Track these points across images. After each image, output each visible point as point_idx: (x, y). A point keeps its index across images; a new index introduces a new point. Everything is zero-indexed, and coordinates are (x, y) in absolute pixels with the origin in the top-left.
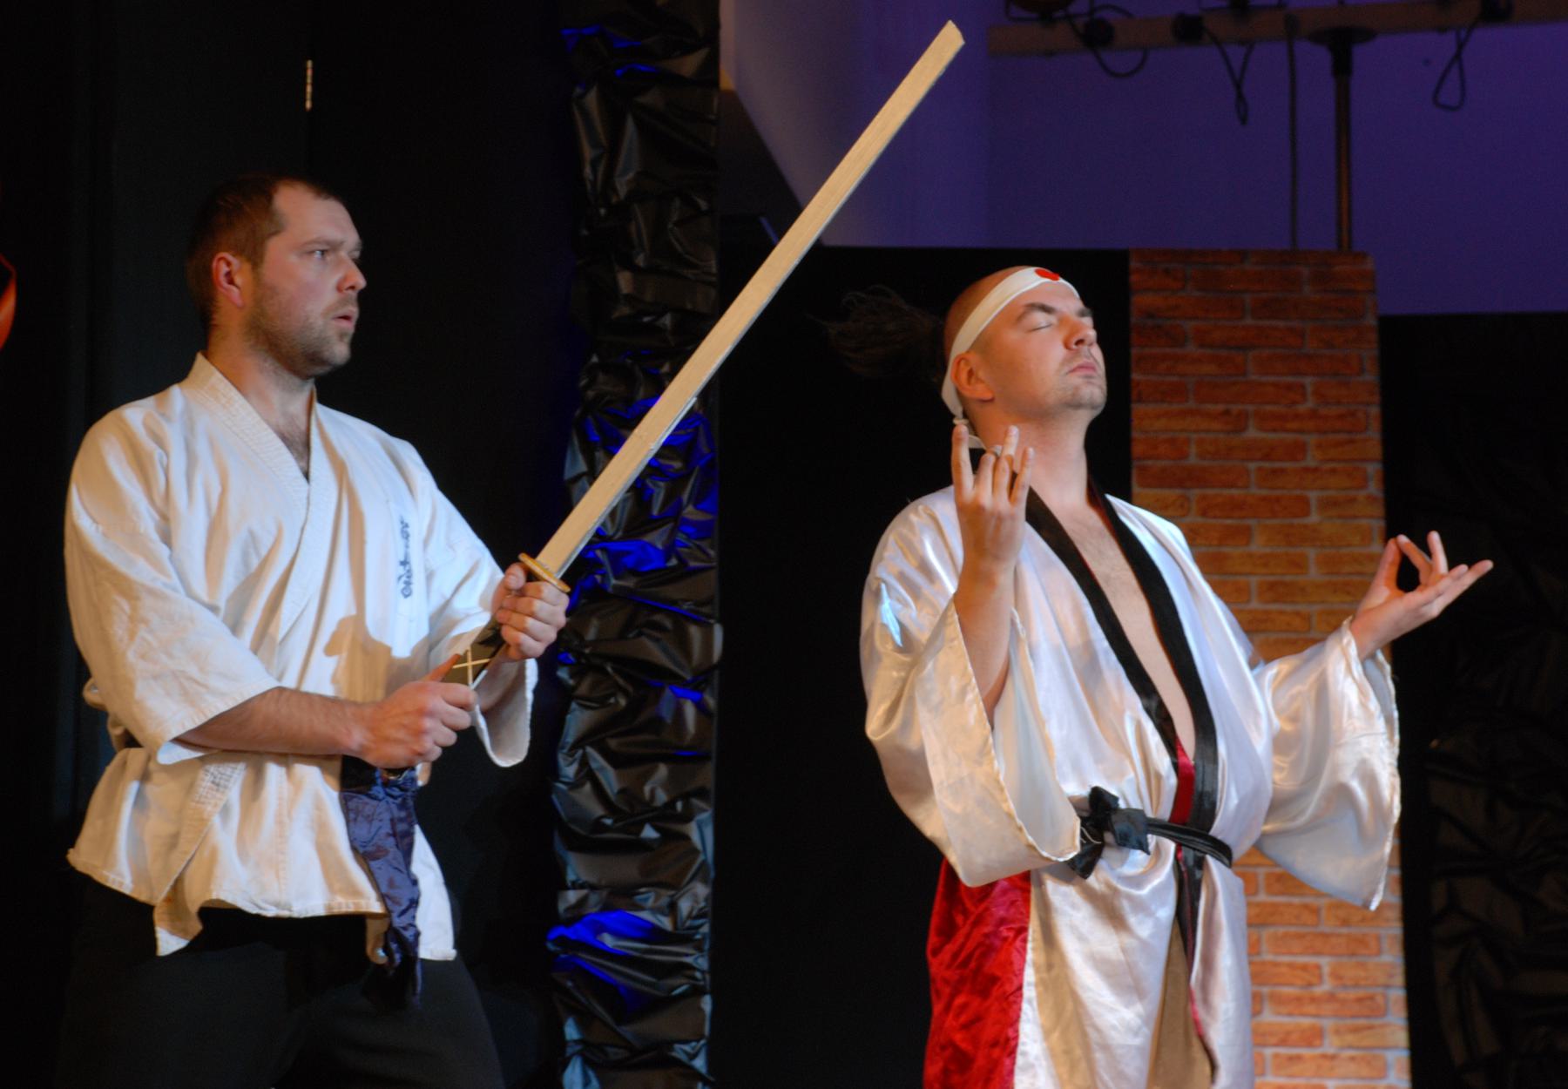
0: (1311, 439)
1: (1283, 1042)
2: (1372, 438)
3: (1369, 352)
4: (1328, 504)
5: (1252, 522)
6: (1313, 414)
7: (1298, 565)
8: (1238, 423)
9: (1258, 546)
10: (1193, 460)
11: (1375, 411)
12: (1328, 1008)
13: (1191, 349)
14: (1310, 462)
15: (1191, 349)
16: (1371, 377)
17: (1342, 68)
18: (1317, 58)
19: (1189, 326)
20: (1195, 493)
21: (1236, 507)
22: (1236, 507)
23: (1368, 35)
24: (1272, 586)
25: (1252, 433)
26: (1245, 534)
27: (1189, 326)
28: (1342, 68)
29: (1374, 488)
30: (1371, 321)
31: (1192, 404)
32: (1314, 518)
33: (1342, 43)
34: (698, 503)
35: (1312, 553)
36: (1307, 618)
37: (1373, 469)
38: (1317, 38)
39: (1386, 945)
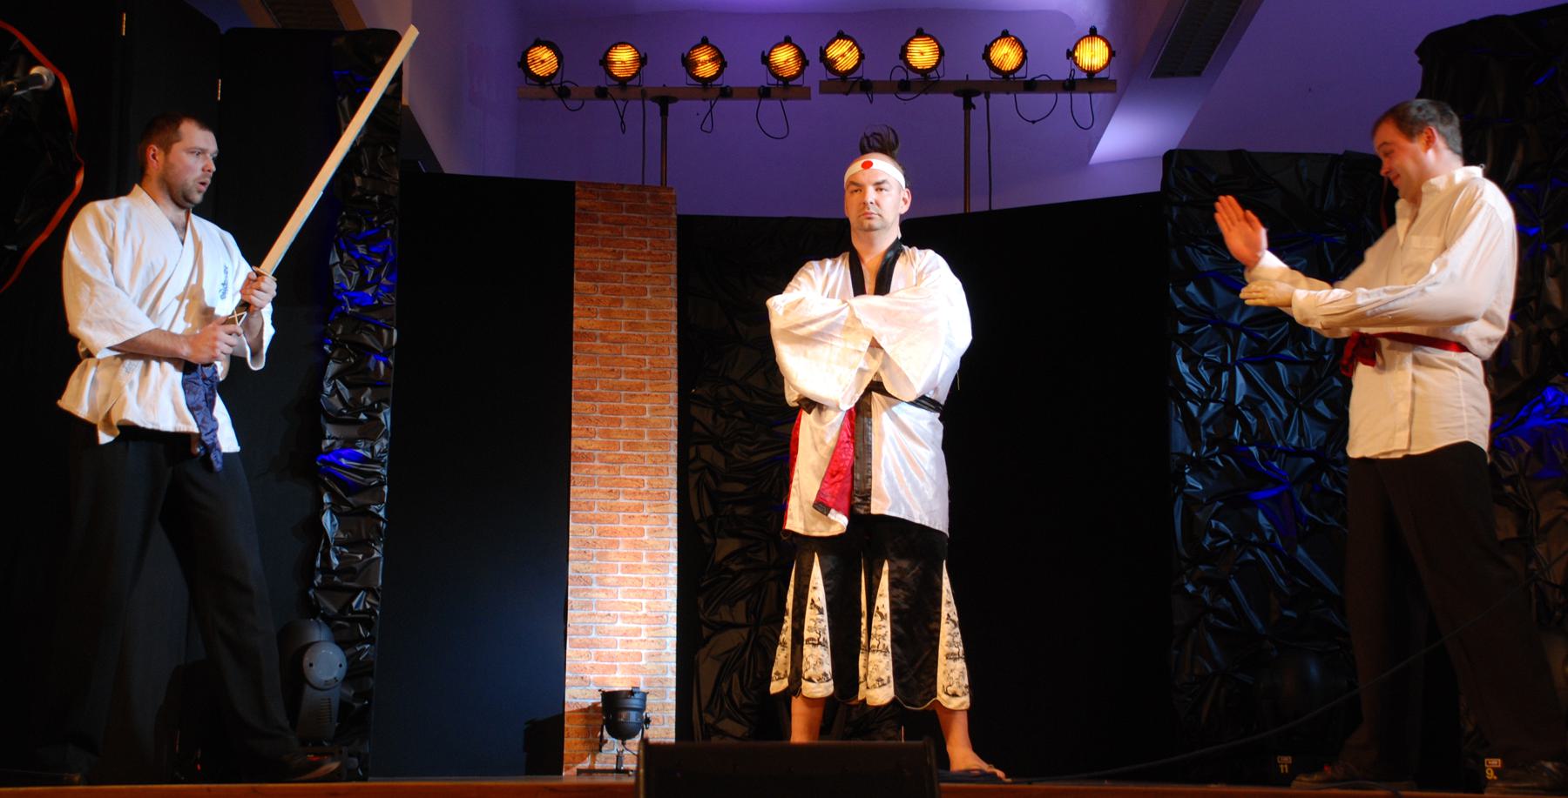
2: (673, 265)
3: (673, 228)
4: (655, 291)
7: (642, 315)
13: (600, 224)
15: (600, 224)
16: (674, 239)
17: (664, 112)
18: (654, 108)
19: (599, 214)
22: (617, 291)
23: (675, 100)
25: (624, 260)
26: (621, 302)
27: (599, 214)
28: (664, 112)
29: (674, 285)
30: (674, 216)
33: (664, 101)
34: (387, 276)
37: (673, 277)
38: (654, 99)
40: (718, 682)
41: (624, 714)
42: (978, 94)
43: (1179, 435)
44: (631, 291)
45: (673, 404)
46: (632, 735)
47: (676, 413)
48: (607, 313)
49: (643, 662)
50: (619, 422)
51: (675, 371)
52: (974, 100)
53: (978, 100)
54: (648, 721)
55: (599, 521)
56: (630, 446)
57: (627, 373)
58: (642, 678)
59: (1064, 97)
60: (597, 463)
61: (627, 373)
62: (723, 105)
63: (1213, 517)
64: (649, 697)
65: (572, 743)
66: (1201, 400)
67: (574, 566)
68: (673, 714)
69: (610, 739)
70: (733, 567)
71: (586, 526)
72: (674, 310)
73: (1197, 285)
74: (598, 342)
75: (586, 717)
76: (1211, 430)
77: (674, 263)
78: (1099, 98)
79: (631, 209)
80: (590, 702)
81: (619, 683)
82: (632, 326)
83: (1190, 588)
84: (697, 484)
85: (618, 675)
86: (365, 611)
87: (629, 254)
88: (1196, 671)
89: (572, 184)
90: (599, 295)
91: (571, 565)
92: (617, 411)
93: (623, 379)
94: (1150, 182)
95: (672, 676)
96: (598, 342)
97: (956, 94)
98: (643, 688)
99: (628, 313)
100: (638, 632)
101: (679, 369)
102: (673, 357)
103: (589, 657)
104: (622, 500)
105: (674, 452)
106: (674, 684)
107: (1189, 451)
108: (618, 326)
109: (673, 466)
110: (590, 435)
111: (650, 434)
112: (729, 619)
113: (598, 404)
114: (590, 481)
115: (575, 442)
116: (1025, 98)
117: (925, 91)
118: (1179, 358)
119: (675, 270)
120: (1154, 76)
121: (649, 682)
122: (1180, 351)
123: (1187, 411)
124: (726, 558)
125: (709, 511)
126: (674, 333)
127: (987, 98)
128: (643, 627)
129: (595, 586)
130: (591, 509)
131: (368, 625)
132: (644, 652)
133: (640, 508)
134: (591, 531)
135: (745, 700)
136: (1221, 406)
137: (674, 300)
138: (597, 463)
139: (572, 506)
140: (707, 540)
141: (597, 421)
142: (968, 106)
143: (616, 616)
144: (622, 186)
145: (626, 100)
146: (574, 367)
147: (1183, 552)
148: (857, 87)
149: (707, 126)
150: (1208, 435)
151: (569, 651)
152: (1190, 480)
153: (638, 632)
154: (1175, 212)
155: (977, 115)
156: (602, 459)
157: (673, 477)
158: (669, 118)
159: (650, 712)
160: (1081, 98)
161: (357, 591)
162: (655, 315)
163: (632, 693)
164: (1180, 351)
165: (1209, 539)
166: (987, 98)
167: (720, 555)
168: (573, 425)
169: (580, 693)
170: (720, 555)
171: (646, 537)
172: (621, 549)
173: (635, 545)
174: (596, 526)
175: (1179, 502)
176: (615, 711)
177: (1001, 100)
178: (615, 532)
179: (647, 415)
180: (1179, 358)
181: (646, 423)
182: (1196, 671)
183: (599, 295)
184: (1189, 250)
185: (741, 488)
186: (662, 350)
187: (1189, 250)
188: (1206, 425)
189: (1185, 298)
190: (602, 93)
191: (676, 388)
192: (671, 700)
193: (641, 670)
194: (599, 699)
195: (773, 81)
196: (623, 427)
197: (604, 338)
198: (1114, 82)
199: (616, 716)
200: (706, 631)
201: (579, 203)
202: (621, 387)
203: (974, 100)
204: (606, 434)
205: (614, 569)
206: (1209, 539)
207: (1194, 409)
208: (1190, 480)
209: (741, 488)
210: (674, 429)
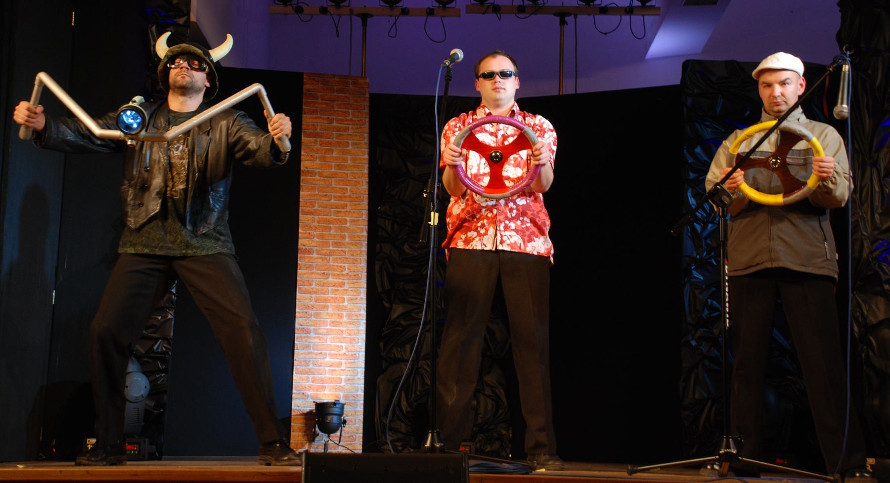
0: (350, 127)
2: (366, 127)
4: (354, 144)
6: (351, 120)
7: (346, 160)
8: (331, 121)
10: (319, 131)
11: (367, 120)
12: (346, 277)
13: (319, 100)
14: (350, 133)
15: (319, 100)
16: (367, 110)
17: (365, 24)
18: (358, 21)
20: (319, 139)
21: (330, 144)
22: (330, 144)
23: (372, 16)
25: (335, 124)
26: (332, 151)
27: (319, 94)
28: (365, 24)
29: (366, 140)
30: (367, 96)
31: (319, 115)
32: (350, 147)
35: (349, 157)
36: (347, 174)
37: (366, 135)
38: (358, 15)
41: (329, 417)
42: (569, 15)
43: (688, 244)
44: (339, 144)
45: (365, 217)
46: (335, 431)
47: (366, 223)
48: (323, 159)
49: (343, 384)
50: (330, 229)
51: (366, 196)
52: (567, 19)
53: (570, 19)
54: (345, 422)
55: (316, 293)
56: (336, 244)
57: (335, 197)
58: (342, 394)
59: (626, 18)
60: (315, 255)
61: (335, 197)
62: (402, 19)
63: (709, 297)
64: (345, 406)
65: (297, 436)
66: (703, 222)
67: (299, 322)
68: (361, 417)
69: (321, 433)
70: (403, 323)
71: (307, 296)
72: (367, 157)
73: (703, 149)
74: (317, 177)
75: (305, 419)
76: (709, 241)
77: (367, 126)
78: (649, 19)
79: (339, 91)
80: (308, 409)
81: (327, 397)
82: (339, 167)
83: (693, 343)
85: (326, 392)
86: (162, 353)
87: (338, 120)
88: (697, 396)
89: (302, 74)
90: (318, 146)
91: (297, 320)
92: (329, 222)
93: (332, 201)
94: (674, 77)
95: (361, 393)
96: (317, 177)
97: (555, 14)
98: (342, 401)
99: (336, 159)
100: (340, 364)
101: (369, 194)
102: (365, 187)
103: (307, 380)
104: (331, 279)
105: (364, 249)
106: (362, 398)
107: (695, 255)
108: (330, 167)
109: (364, 257)
110: (310, 237)
111: (350, 237)
112: (400, 356)
113: (316, 217)
114: (310, 267)
115: (301, 242)
116: (600, 18)
117: (535, 13)
118: (689, 194)
119: (367, 131)
120: (685, 4)
121: (346, 397)
122: (690, 190)
123: (694, 229)
124: (398, 317)
125: (387, 286)
126: (366, 171)
127: (575, 17)
128: (343, 361)
129: (312, 335)
130: (311, 285)
131: (164, 361)
132: (343, 377)
134: (311, 299)
135: (409, 409)
136: (716, 226)
137: (367, 150)
138: (315, 255)
140: (387, 305)
142: (563, 23)
143: (325, 354)
144: (334, 76)
145: (340, 16)
146: (302, 193)
147: (689, 320)
148: (490, 9)
149: (393, 33)
150: (707, 245)
151: (296, 377)
152: (695, 274)
153: (340, 364)
154: (690, 101)
155: (569, 28)
156: (318, 253)
157: (364, 265)
158: (368, 28)
159: (345, 417)
160: (637, 19)
161: (157, 340)
162: (354, 160)
163: (335, 404)
164: (690, 190)
165: (706, 312)
166: (575, 17)
167: (394, 315)
170: (394, 315)
171: (346, 303)
172: (330, 311)
174: (314, 296)
175: (687, 289)
176: (324, 417)
177: (585, 20)
178: (326, 300)
179: (348, 225)
180: (689, 194)
181: (347, 229)
182: (697, 396)
183: (318, 146)
184: (697, 125)
185: (411, 271)
186: (358, 182)
187: (697, 125)
188: (706, 238)
189: (694, 155)
190: (324, 11)
191: (367, 207)
192: (360, 408)
194: (313, 408)
195: (437, 5)
196: (332, 232)
197: (321, 175)
198: (659, 8)
199: (324, 418)
201: (306, 87)
202: (331, 206)
203: (567, 19)
204: (321, 236)
205: (325, 323)
206: (706, 312)
207: (698, 228)
208: (695, 274)
209: (411, 271)
210: (365, 234)
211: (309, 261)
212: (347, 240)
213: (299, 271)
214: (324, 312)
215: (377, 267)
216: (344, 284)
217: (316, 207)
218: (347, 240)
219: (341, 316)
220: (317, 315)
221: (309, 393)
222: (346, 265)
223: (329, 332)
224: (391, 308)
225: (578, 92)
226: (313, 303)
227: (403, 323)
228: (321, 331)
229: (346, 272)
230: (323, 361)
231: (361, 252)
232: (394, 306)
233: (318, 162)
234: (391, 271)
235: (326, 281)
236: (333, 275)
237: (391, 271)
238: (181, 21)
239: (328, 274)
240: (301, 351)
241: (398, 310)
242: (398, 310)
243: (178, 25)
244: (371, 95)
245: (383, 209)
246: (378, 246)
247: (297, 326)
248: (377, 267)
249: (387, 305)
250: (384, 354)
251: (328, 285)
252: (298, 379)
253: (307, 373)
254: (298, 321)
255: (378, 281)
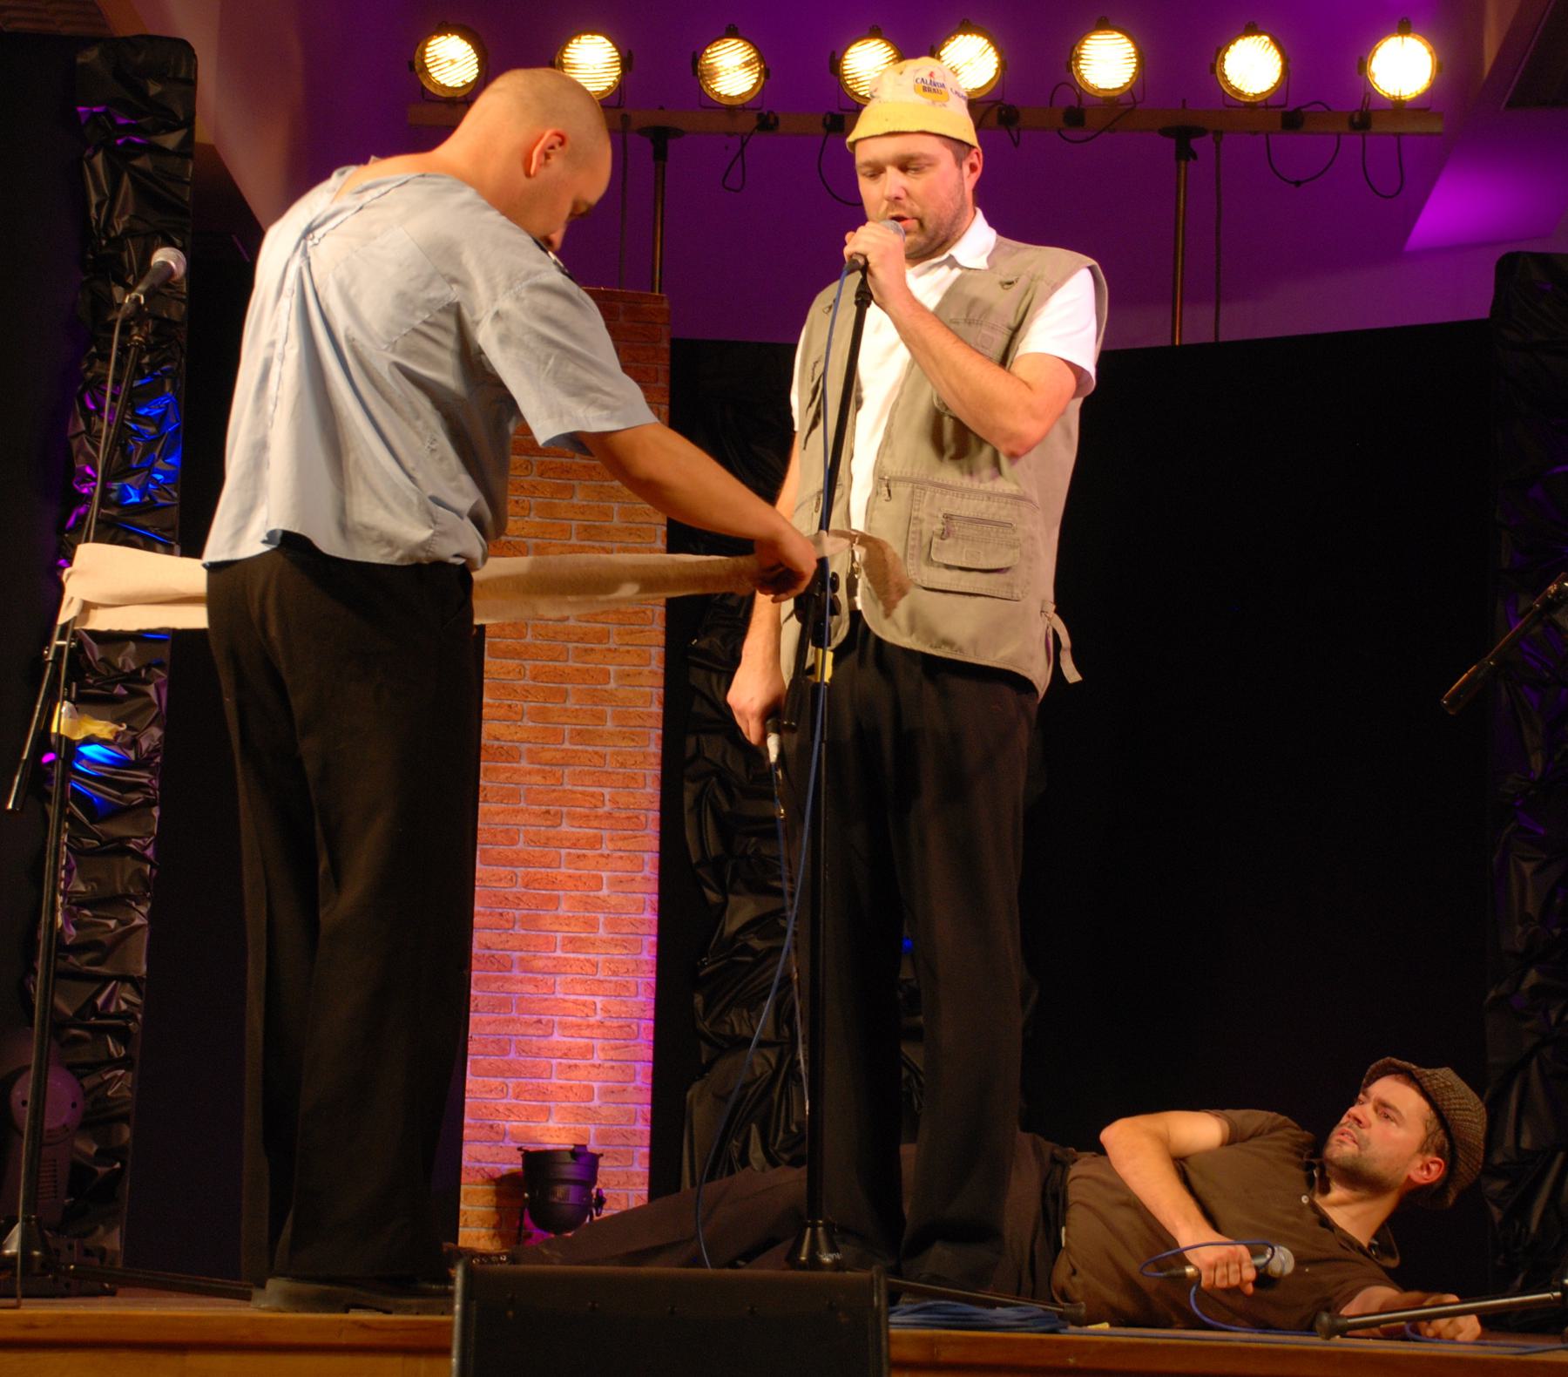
1: (574, 846)
5: (575, 483)
7: (607, 515)
9: (577, 500)
24: (586, 528)
30: (665, 344)
35: (616, 507)
39: (649, 781)
40: (724, 1138)
49: (596, 1102)
50: (564, 695)
55: (527, 863)
56: (581, 736)
58: (593, 1130)
60: (524, 764)
64: (602, 1162)
67: (482, 939)
69: (536, 1232)
70: (757, 944)
71: (504, 871)
75: (498, 1193)
80: (506, 1168)
81: (555, 1133)
84: (698, 800)
85: (552, 1124)
90: (534, 478)
91: (476, 935)
92: (561, 676)
94: (1477, 303)
98: (593, 1147)
100: (588, 1051)
104: (565, 828)
105: (655, 748)
113: (528, 664)
114: (512, 796)
121: (603, 1136)
125: (714, 847)
128: (598, 1043)
129: (517, 973)
130: (513, 842)
131: (123, 1036)
132: (596, 1085)
133: (595, 842)
134: (513, 880)
138: (524, 764)
139: (481, 837)
140: (712, 896)
141: (526, 694)
143: (551, 1024)
151: (472, 1082)
153: (588, 1051)
156: (533, 757)
167: (733, 924)
168: (486, 700)
169: (484, 1155)
170: (733, 924)
171: (605, 892)
172: (563, 910)
173: (586, 904)
174: (520, 871)
176: (545, 1187)
178: (552, 883)
191: (661, 639)
193: (588, 1115)
196: (571, 704)
200: (705, 1052)
204: (541, 715)
205: (550, 944)
210: (657, 709)
211: (508, 780)
212: (610, 725)
213: (483, 807)
214: (547, 916)
215: (688, 798)
216: (600, 840)
217: (529, 639)
218: (610, 725)
219: (591, 925)
220: (531, 922)
221: (508, 1125)
222: (606, 791)
223: (558, 968)
224: (724, 906)
225: (1221, 339)
226: (519, 889)
227: (757, 944)
228: (539, 964)
229: (607, 808)
230: (544, 1042)
231: (645, 756)
232: (732, 899)
233: (534, 518)
234: (726, 808)
235: (552, 831)
236: (572, 816)
237: (726, 808)
238: (171, 141)
239: (559, 815)
240: (486, 1017)
241: (742, 911)
242: (742, 911)
243: (162, 151)
244: (673, 342)
245: (704, 644)
246: (691, 742)
247: (476, 950)
248: (688, 798)
249: (712, 896)
250: (704, 1026)
251: (561, 842)
252: (482, 1089)
253: (500, 1073)
254: (479, 937)
255: (690, 836)
